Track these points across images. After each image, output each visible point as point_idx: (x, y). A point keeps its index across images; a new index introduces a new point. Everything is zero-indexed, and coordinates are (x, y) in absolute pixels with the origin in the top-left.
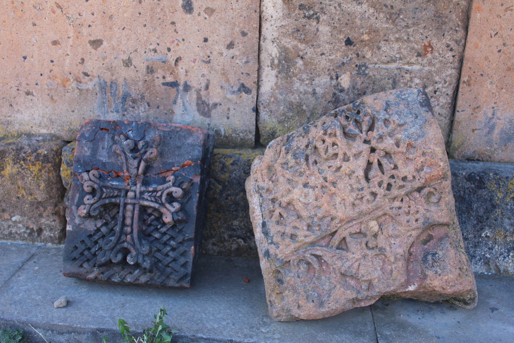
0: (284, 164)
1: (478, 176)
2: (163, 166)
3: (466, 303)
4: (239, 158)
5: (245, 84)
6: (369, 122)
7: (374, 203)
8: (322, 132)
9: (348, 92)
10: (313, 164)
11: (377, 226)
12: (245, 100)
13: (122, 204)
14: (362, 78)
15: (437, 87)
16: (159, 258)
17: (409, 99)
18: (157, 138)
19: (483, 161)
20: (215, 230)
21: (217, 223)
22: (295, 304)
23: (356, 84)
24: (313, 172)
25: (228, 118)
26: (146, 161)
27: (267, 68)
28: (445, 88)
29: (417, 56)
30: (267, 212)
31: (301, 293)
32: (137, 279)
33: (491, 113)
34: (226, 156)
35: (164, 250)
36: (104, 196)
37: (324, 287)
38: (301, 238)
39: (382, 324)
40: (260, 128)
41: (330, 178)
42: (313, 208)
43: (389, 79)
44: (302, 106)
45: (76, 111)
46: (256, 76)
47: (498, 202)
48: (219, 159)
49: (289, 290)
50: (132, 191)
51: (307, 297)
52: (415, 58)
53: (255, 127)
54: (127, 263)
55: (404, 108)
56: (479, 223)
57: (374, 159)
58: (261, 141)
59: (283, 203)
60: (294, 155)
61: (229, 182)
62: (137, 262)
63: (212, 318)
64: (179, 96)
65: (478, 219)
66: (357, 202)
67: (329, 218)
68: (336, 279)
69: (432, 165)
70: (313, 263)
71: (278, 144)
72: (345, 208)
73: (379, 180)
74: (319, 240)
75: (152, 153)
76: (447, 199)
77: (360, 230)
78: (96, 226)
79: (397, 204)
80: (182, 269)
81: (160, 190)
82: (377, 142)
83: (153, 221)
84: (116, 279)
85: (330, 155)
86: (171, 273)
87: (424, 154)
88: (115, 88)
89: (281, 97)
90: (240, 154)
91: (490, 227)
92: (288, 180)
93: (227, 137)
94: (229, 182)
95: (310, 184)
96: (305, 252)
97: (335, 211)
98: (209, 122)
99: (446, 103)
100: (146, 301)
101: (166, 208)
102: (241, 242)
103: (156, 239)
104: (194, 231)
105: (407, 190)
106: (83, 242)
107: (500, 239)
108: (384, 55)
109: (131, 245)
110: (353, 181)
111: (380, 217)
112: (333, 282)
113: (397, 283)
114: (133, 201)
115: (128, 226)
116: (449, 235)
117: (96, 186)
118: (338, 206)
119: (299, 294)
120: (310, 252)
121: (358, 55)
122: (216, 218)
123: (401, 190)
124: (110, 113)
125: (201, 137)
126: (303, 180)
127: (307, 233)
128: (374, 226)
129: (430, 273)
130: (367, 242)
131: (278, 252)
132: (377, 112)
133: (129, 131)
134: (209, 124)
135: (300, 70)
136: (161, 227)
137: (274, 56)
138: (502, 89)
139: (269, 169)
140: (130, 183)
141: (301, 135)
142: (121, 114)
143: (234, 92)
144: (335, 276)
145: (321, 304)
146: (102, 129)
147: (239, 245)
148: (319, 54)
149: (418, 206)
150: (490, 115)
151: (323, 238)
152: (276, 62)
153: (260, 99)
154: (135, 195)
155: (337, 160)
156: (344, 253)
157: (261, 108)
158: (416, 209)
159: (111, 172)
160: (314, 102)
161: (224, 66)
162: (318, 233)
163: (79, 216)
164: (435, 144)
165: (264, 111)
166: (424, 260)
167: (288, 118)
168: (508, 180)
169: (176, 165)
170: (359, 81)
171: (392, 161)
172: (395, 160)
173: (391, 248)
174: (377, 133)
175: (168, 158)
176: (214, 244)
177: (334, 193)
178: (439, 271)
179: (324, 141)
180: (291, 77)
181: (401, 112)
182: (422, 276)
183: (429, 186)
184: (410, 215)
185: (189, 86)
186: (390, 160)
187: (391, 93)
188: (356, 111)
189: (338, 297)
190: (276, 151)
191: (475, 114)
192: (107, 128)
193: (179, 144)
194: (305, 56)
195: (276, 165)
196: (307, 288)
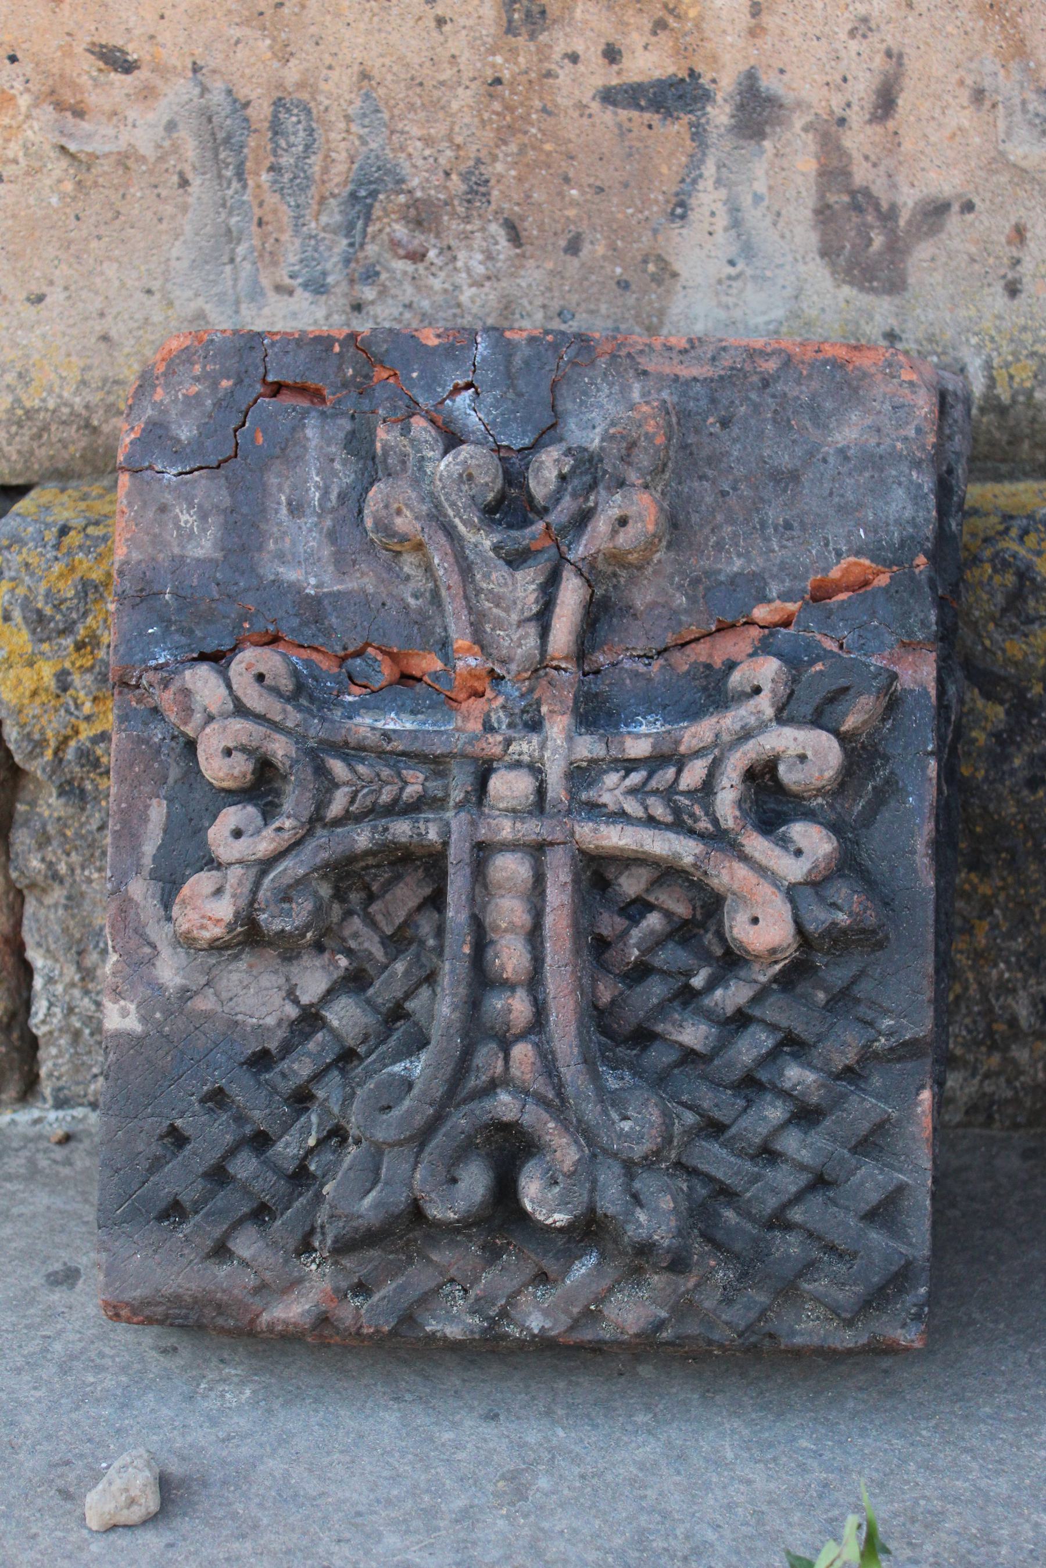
2: (692, 600)
13: (458, 852)
16: (719, 1175)
18: (650, 427)
25: (1013, 290)
26: (590, 575)
32: (590, 1316)
35: (744, 1122)
36: (336, 808)
45: (56, 296)
50: (517, 765)
54: (524, 1216)
62: (592, 1209)
64: (709, 169)
75: (623, 521)
78: (291, 996)
80: (873, 1235)
81: (698, 754)
83: (659, 942)
84: (452, 1319)
86: (809, 1267)
88: (300, 139)
93: (1002, 410)
98: (893, 322)
100: (647, 1449)
101: (745, 858)
103: (689, 1056)
106: (217, 1098)
109: (542, 1101)
114: (532, 829)
115: (509, 986)
117: (280, 748)
124: (272, 297)
125: (924, 405)
133: (457, 390)
134: (891, 337)
136: (712, 985)
140: (499, 719)
142: (338, 299)
146: (277, 389)
154: (541, 791)
159: (359, 653)
163: (186, 942)
169: (774, 589)
175: (719, 546)
185: (772, 101)
192: (313, 381)
193: (785, 460)
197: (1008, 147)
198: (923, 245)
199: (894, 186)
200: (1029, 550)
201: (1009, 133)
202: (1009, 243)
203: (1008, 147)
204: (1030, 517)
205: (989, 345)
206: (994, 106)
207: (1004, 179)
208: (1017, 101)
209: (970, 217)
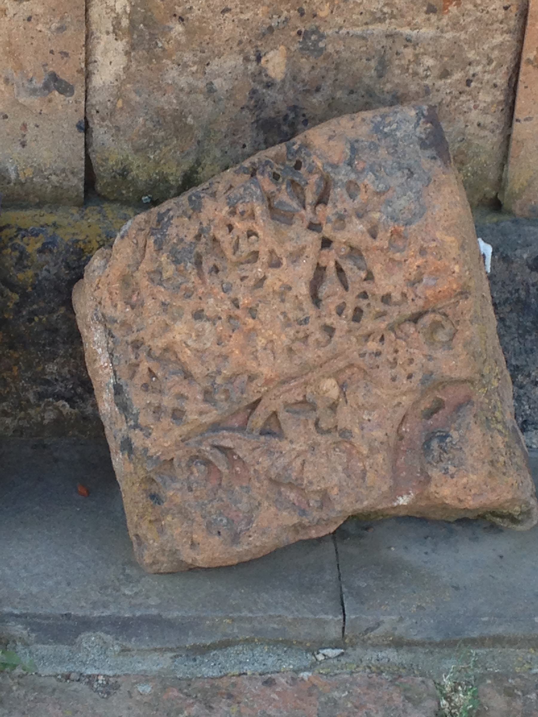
0: (154, 272)
3: (513, 520)
4: (54, 237)
5: (59, 73)
6: (319, 186)
7: (329, 347)
9: (283, 86)
10: (210, 272)
12: (60, 107)
14: (312, 59)
15: (471, 72)
17: (398, 134)
21: (10, 369)
22: (185, 540)
23: (300, 71)
24: (212, 289)
25: (23, 145)
27: (104, 37)
28: (489, 72)
29: (427, 12)
31: (197, 519)
38: (192, 417)
40: (93, 161)
41: (244, 301)
42: (214, 359)
43: (368, 60)
44: (186, 118)
46: (83, 56)
48: (11, 239)
49: (173, 515)
51: (209, 525)
52: (424, 16)
53: (83, 162)
57: (328, 261)
60: (174, 256)
61: (34, 287)
63: (24, 574)
66: (296, 346)
67: (245, 377)
69: (437, 270)
70: (217, 464)
72: (274, 358)
76: (467, 333)
77: (305, 396)
79: (373, 346)
82: (335, 229)
87: (422, 251)
89: (138, 99)
92: (163, 304)
93: (22, 184)
94: (34, 287)
95: (207, 313)
96: (200, 443)
97: (254, 364)
99: (492, 103)
108: (357, 10)
111: (341, 371)
113: (375, 494)
116: (474, 399)
119: (193, 521)
120: (210, 441)
121: (302, 12)
122: (7, 360)
126: (191, 305)
129: (435, 473)
131: (148, 443)
135: (178, 43)
137: (119, 8)
139: (123, 280)
141: (184, 213)
143: (34, 92)
144: (258, 485)
145: (235, 538)
148: (219, 10)
149: (412, 350)
151: (235, 414)
152: (125, 22)
153: (93, 101)
156: (274, 441)
158: (408, 356)
161: (9, 36)
162: (225, 406)
164: (445, 229)
165: (101, 126)
166: (425, 449)
167: (156, 143)
170: (305, 64)
171: (362, 264)
172: (369, 264)
177: (254, 329)
178: (452, 469)
179: (231, 228)
180: (159, 59)
181: (380, 166)
182: (422, 479)
183: (434, 311)
186: (359, 262)
187: (363, 120)
188: (294, 163)
190: (137, 244)
194: (188, 15)
195: (138, 274)
201: (19, 93)
202: (21, 129)
203: (19, 98)
204: (26, 230)
205: (16, 163)
206: (13, 84)
207: (18, 108)
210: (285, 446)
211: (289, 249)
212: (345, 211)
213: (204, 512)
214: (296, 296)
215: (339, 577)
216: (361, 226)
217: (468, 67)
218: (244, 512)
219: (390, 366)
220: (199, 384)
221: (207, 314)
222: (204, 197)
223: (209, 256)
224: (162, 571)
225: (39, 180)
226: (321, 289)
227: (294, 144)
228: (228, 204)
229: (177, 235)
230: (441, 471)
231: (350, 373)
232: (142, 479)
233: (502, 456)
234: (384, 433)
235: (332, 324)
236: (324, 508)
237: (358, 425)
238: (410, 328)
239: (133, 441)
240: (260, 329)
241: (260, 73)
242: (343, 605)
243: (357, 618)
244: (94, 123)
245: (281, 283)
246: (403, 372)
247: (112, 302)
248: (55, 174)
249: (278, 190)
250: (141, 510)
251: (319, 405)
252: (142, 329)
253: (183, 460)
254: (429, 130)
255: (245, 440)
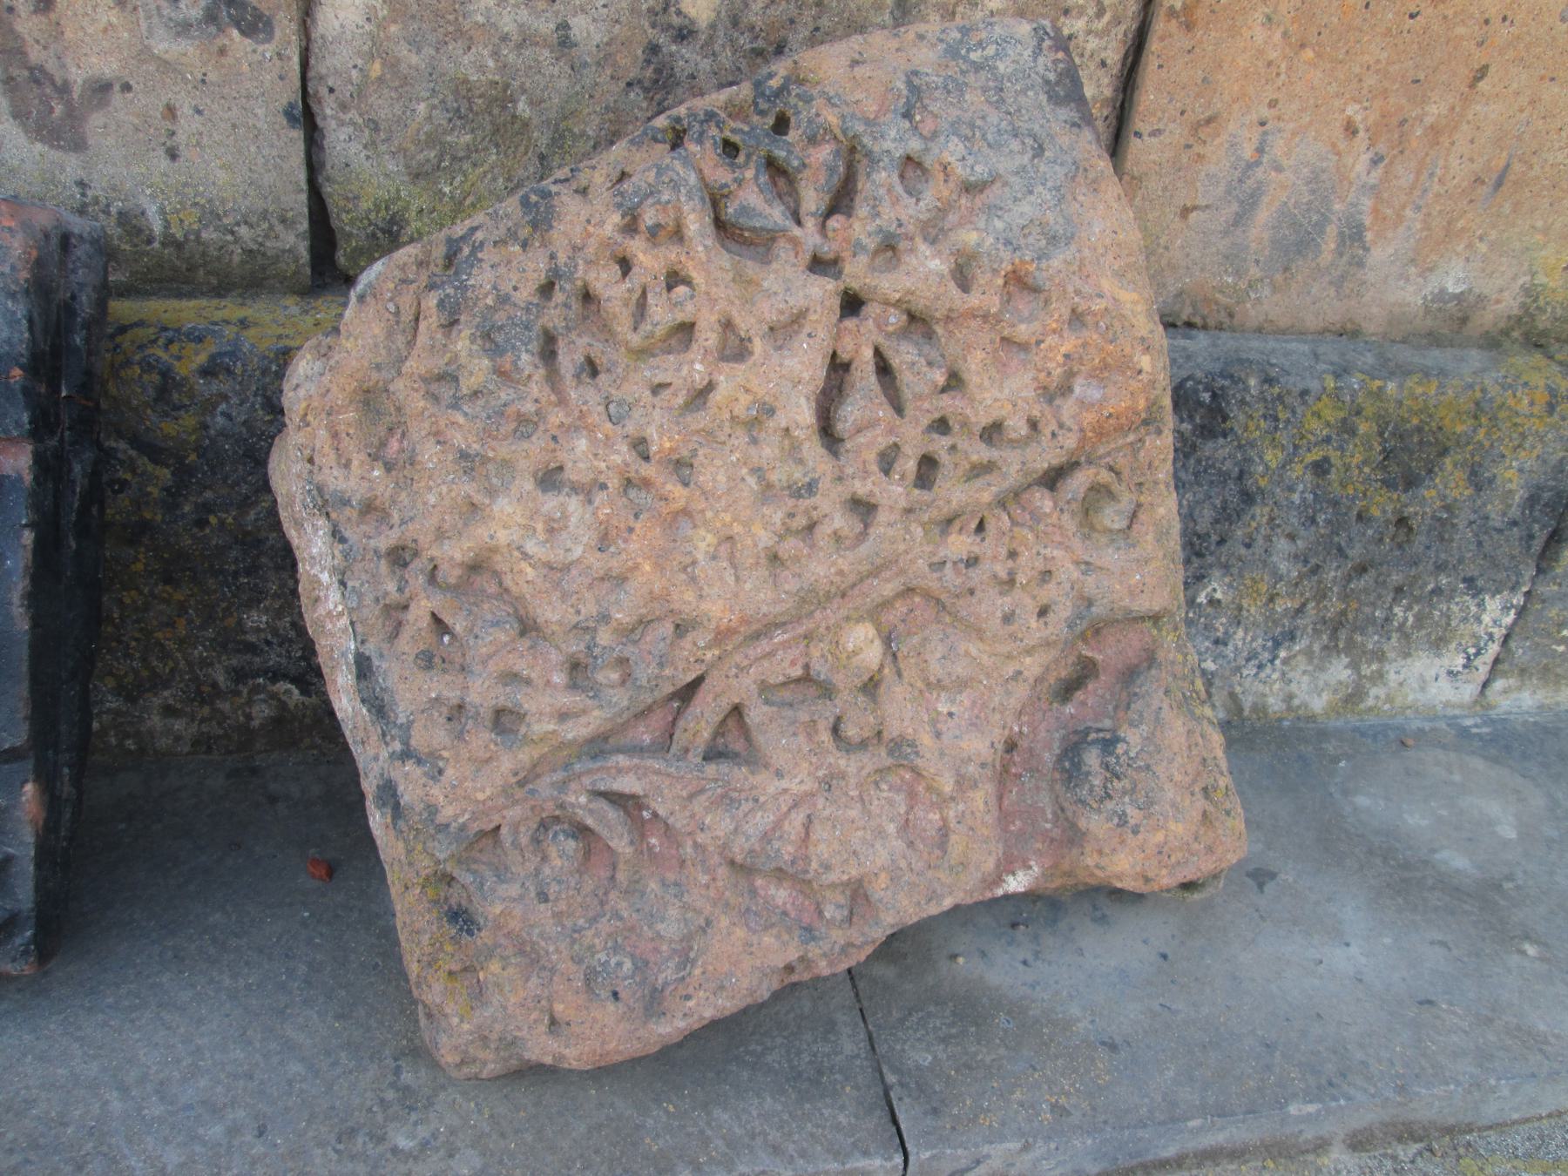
0: (440, 378)
1: (1206, 389)
4: (236, 343)
6: (832, 170)
7: (864, 549)
8: (616, 218)
10: (577, 376)
11: (877, 642)
12: (245, 67)
17: (1001, 67)
19: (1205, 327)
20: (165, 655)
21: (171, 624)
24: (582, 415)
30: (371, 612)
31: (562, 966)
33: (1255, 143)
34: (173, 335)
37: (660, 927)
39: (896, 1014)
40: (329, 202)
41: (659, 443)
44: (514, 101)
47: (1262, 483)
48: (141, 347)
51: (590, 978)
53: (304, 197)
55: (985, 107)
56: (1194, 559)
57: (858, 346)
58: (341, 259)
59: (444, 567)
60: (487, 336)
65: (1192, 544)
66: (790, 546)
67: (667, 628)
68: (712, 893)
70: (604, 833)
71: (403, 281)
72: (737, 579)
73: (883, 442)
74: (625, 726)
77: (807, 667)
79: (959, 544)
85: (660, 332)
87: (1077, 318)
89: (414, 59)
90: (244, 324)
91: (1226, 567)
92: (464, 455)
93: (179, 246)
94: (198, 448)
95: (570, 474)
96: (563, 786)
98: (81, 173)
102: (288, 692)
104: (23, 710)
105: (1006, 485)
107: (1253, 609)
110: (768, 451)
111: (886, 604)
112: (699, 904)
116: (1160, 655)
118: (704, 567)
119: (553, 970)
120: (586, 781)
122: (163, 607)
123: (979, 483)
126: (532, 453)
127: (567, 700)
128: (863, 643)
129: (1095, 823)
130: (838, 719)
131: (437, 793)
132: (868, 122)
134: (81, 184)
138: (1303, 46)
139: (367, 403)
144: (704, 879)
145: (654, 1003)
147: (283, 706)
149: (1048, 552)
150: (1248, 152)
151: (644, 714)
153: (319, 67)
155: (690, 355)
157: (328, 110)
158: (1040, 565)
160: (564, 83)
162: (621, 698)
165: (342, 124)
166: (1064, 770)
167: (454, 158)
168: (1305, 403)
171: (934, 355)
172: (953, 349)
173: (938, 735)
174: (871, 228)
176: (169, 711)
177: (686, 512)
179: (625, 265)
181: (972, 126)
182: (1056, 833)
184: (1017, 593)
186: (926, 349)
187: (921, 37)
188: (771, 121)
189: (726, 967)
190: (397, 313)
191: (1198, 149)
195: (399, 386)
196: (586, 942)
197: (152, 42)
198: (95, 115)
199: (64, 66)
200: (172, 356)
201: (150, 30)
202: (163, 118)
203: (152, 42)
205: (161, 197)
206: (135, 9)
208: (153, 7)
209: (130, 96)
210: (770, 786)
211: (767, 315)
212: (900, 225)
213: (576, 947)
214: (787, 430)
215: (870, 1038)
216: (937, 261)
217: (1062, 19)
218: (671, 941)
219: (997, 590)
220: (557, 647)
221: (574, 477)
222: (558, 194)
223: (573, 336)
224: (484, 1076)
225: (214, 236)
226: (841, 413)
227: (771, 76)
228: (619, 206)
229: (495, 288)
230: (1109, 819)
231: (904, 610)
232: (427, 879)
233: (1222, 773)
234: (988, 744)
235: (871, 493)
236: (855, 919)
237: (928, 729)
238: (1043, 501)
239: (401, 788)
240: (702, 511)
241: (665, 10)
242: (895, 1121)
243: (933, 1157)
244: (325, 118)
245: (750, 398)
246: (1028, 601)
247: (339, 456)
248: (246, 223)
249: (735, 180)
250: (428, 950)
251: (841, 686)
252: (412, 519)
253: (523, 829)
254: (1061, 66)
255: (669, 775)
